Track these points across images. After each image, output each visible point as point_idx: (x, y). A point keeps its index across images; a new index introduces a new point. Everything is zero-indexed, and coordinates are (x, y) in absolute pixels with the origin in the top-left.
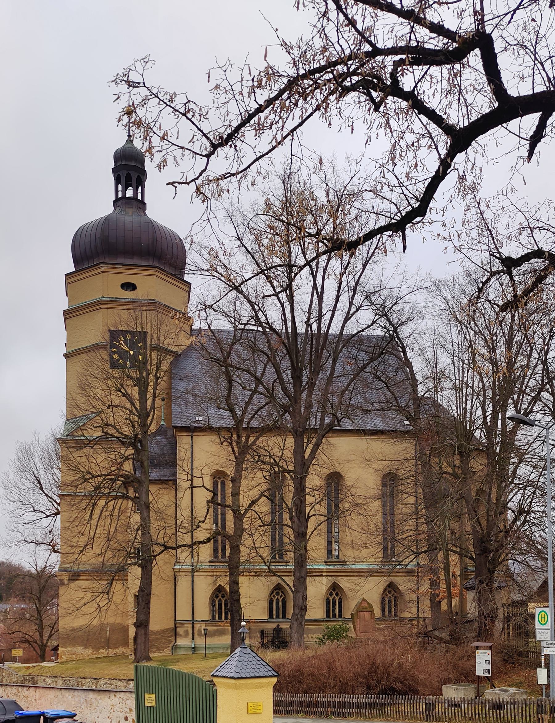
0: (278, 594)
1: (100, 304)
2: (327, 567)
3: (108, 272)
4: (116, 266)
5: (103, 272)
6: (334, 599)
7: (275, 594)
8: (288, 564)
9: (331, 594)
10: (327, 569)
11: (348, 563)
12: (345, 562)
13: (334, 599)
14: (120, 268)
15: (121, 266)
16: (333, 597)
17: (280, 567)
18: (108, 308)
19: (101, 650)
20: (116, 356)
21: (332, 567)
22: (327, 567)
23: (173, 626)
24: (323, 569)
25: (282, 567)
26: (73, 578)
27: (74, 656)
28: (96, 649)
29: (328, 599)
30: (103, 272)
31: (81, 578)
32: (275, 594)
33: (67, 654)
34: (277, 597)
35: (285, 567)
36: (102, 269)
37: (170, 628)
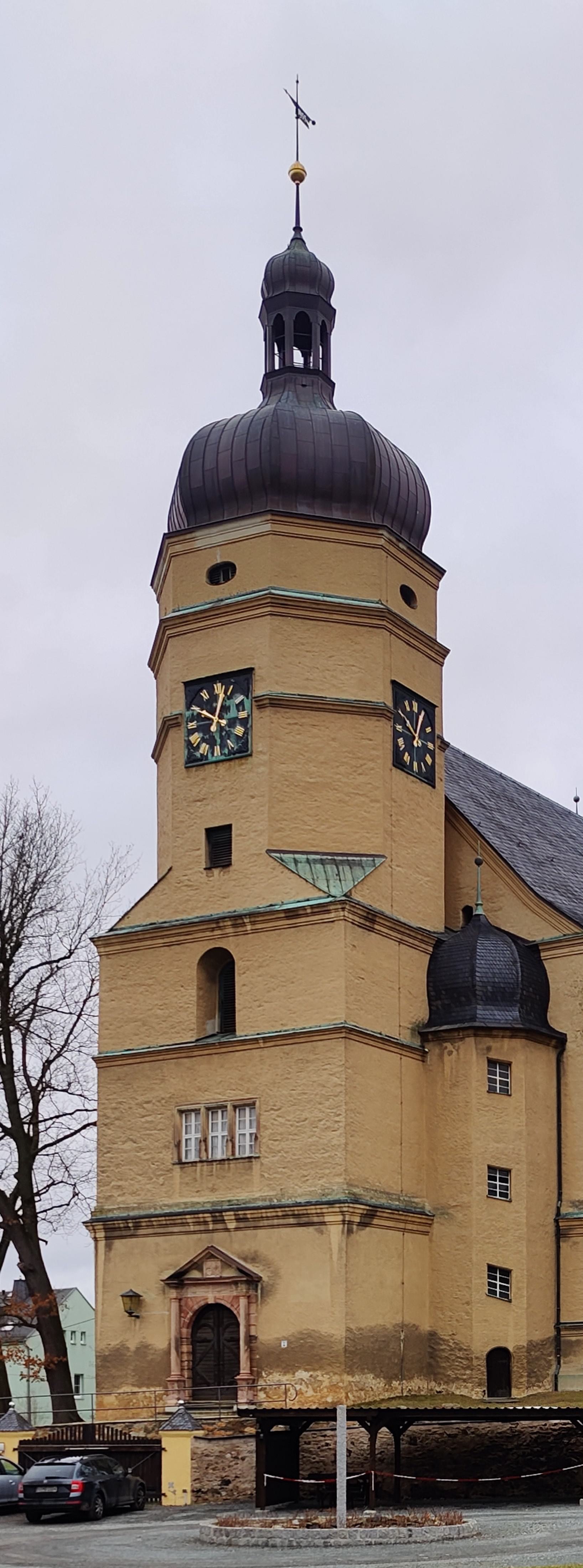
1: (382, 617)
3: (388, 552)
4: (401, 545)
5: (382, 547)
14: (402, 551)
18: (391, 632)
19: (395, 1383)
20: (401, 741)
23: (552, 1333)
26: (367, 1220)
27: (362, 1393)
28: (389, 1379)
30: (382, 547)
31: (375, 1221)
33: (354, 1388)
36: (382, 542)
37: (549, 1338)
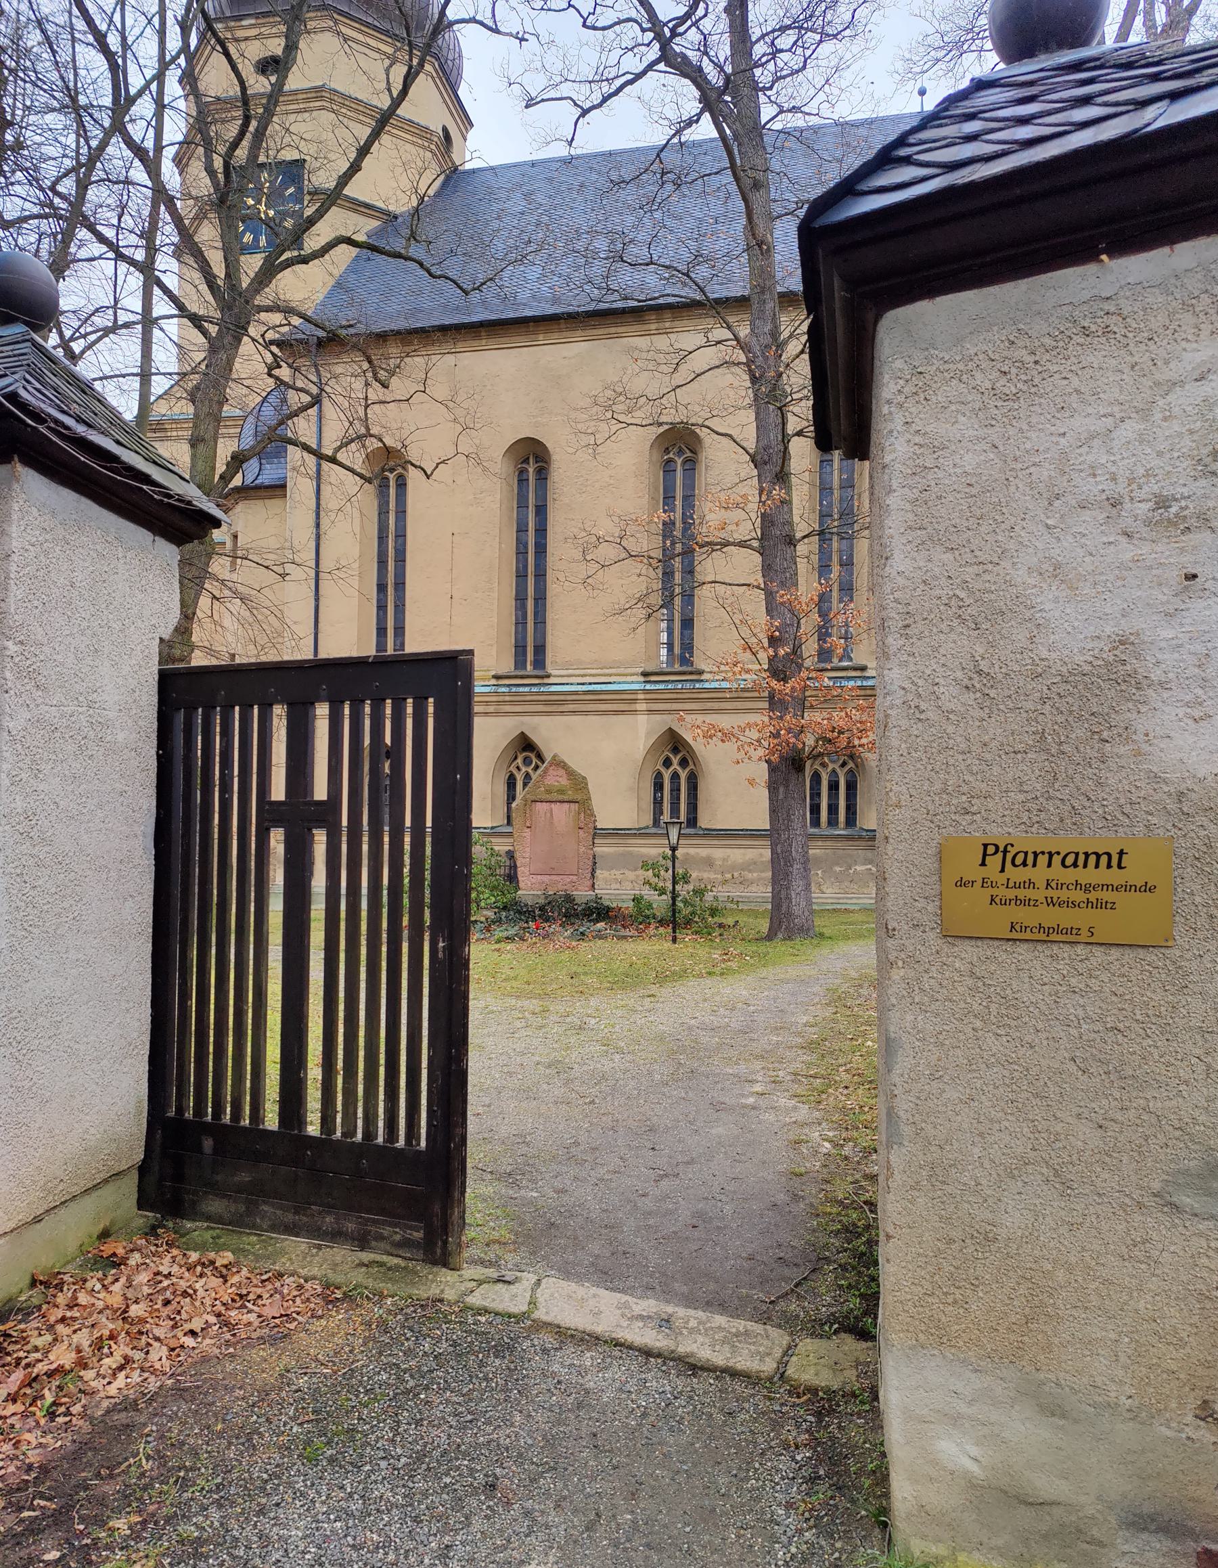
0: (527, 762)
2: (648, 687)
6: (675, 776)
7: (519, 761)
8: (546, 681)
9: (667, 763)
10: (646, 691)
11: (705, 677)
12: (701, 673)
13: (675, 776)
15: (253, 21)
16: (671, 769)
17: (521, 689)
21: (662, 686)
22: (648, 687)
24: (635, 692)
25: (527, 689)
29: (659, 775)
32: (519, 761)
34: (524, 769)
35: (535, 689)
